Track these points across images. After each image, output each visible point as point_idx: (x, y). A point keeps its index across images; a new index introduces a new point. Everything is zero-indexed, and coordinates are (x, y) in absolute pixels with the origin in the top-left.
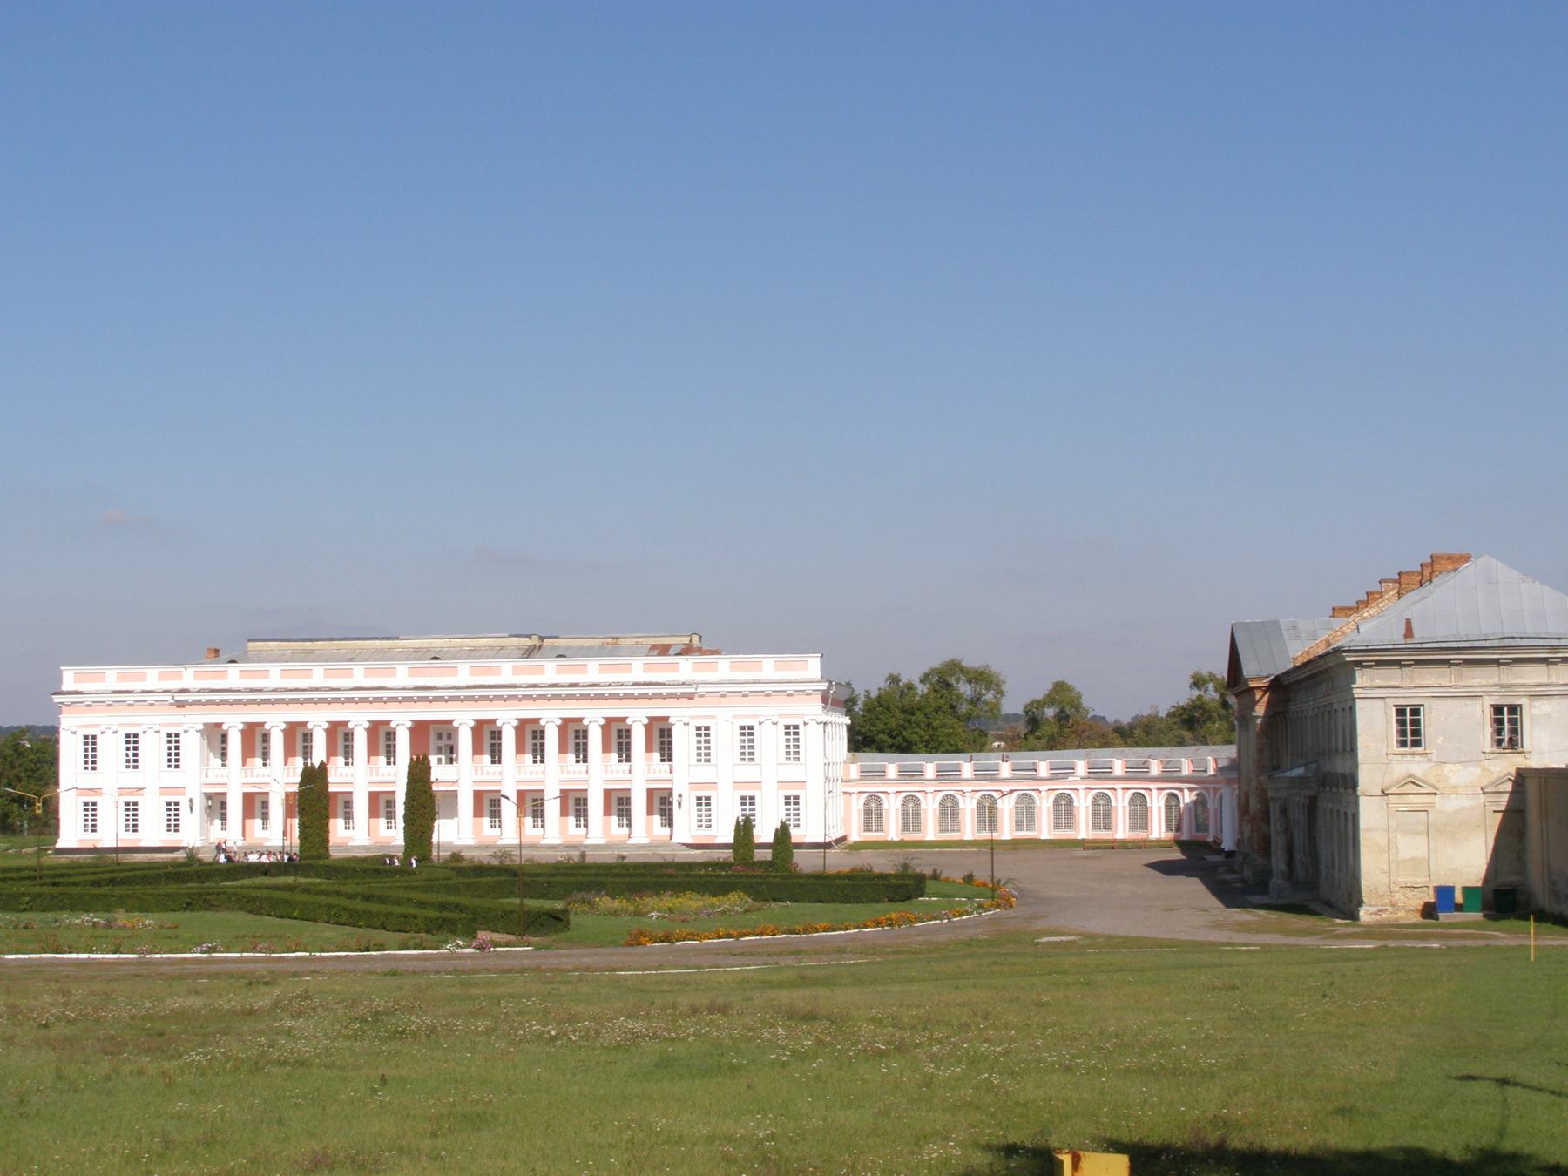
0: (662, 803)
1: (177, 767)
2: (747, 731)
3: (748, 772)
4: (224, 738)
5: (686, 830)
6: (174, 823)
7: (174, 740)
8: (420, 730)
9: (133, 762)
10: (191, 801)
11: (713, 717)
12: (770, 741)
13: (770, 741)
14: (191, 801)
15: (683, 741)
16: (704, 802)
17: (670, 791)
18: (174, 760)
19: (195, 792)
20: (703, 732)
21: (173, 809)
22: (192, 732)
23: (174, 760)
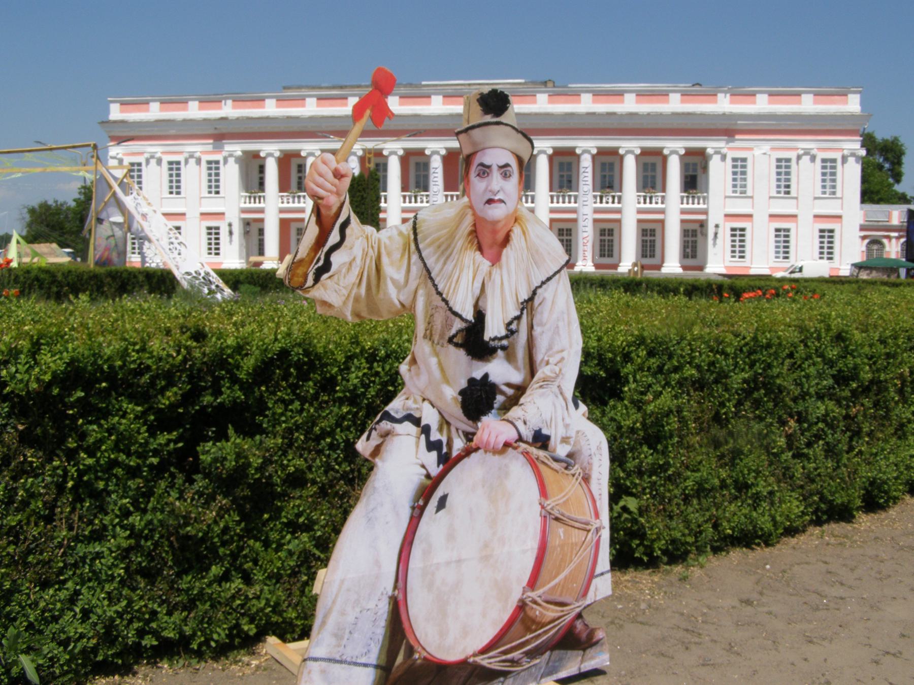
0: (694, 237)
1: (217, 193)
2: (783, 167)
3: (784, 207)
4: (262, 169)
5: (718, 263)
6: (214, 247)
7: (213, 166)
8: (450, 158)
9: (175, 187)
10: (230, 225)
11: (751, 149)
12: (806, 176)
13: (806, 176)
14: (230, 225)
15: (719, 174)
16: (739, 234)
17: (703, 224)
18: (214, 187)
19: (234, 217)
20: (740, 167)
21: (213, 233)
22: (231, 160)
23: (214, 187)
